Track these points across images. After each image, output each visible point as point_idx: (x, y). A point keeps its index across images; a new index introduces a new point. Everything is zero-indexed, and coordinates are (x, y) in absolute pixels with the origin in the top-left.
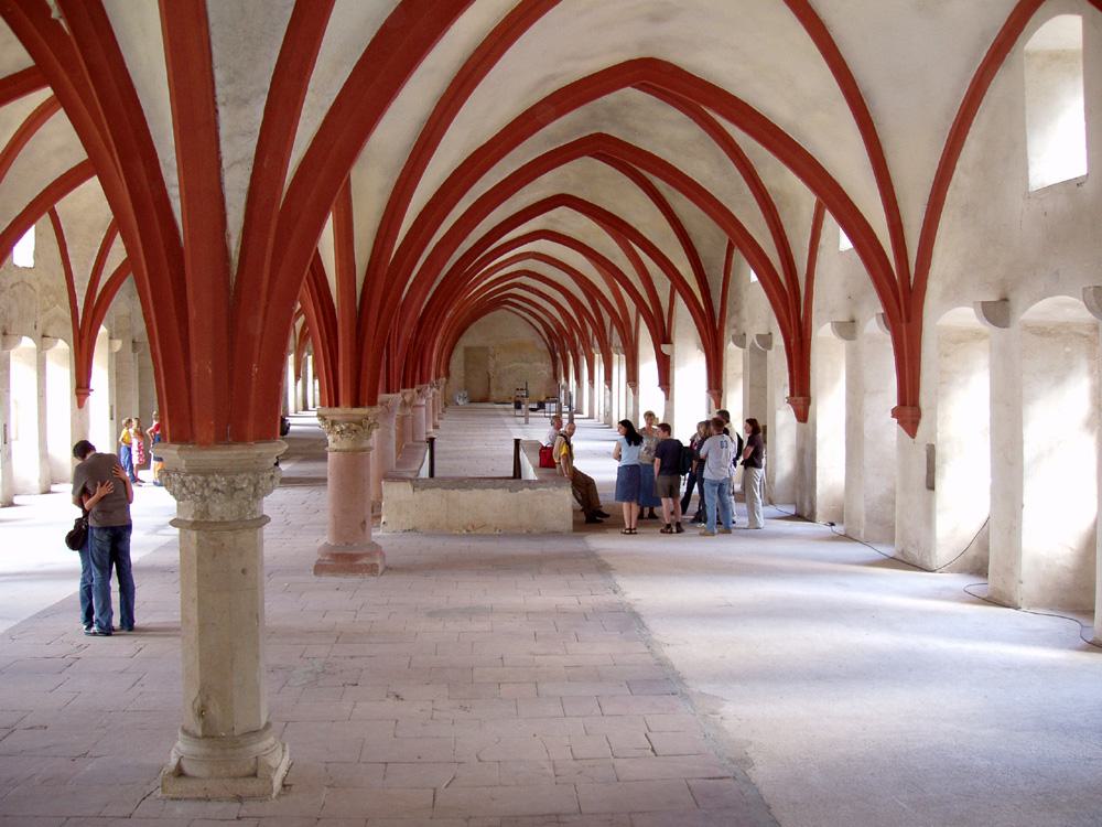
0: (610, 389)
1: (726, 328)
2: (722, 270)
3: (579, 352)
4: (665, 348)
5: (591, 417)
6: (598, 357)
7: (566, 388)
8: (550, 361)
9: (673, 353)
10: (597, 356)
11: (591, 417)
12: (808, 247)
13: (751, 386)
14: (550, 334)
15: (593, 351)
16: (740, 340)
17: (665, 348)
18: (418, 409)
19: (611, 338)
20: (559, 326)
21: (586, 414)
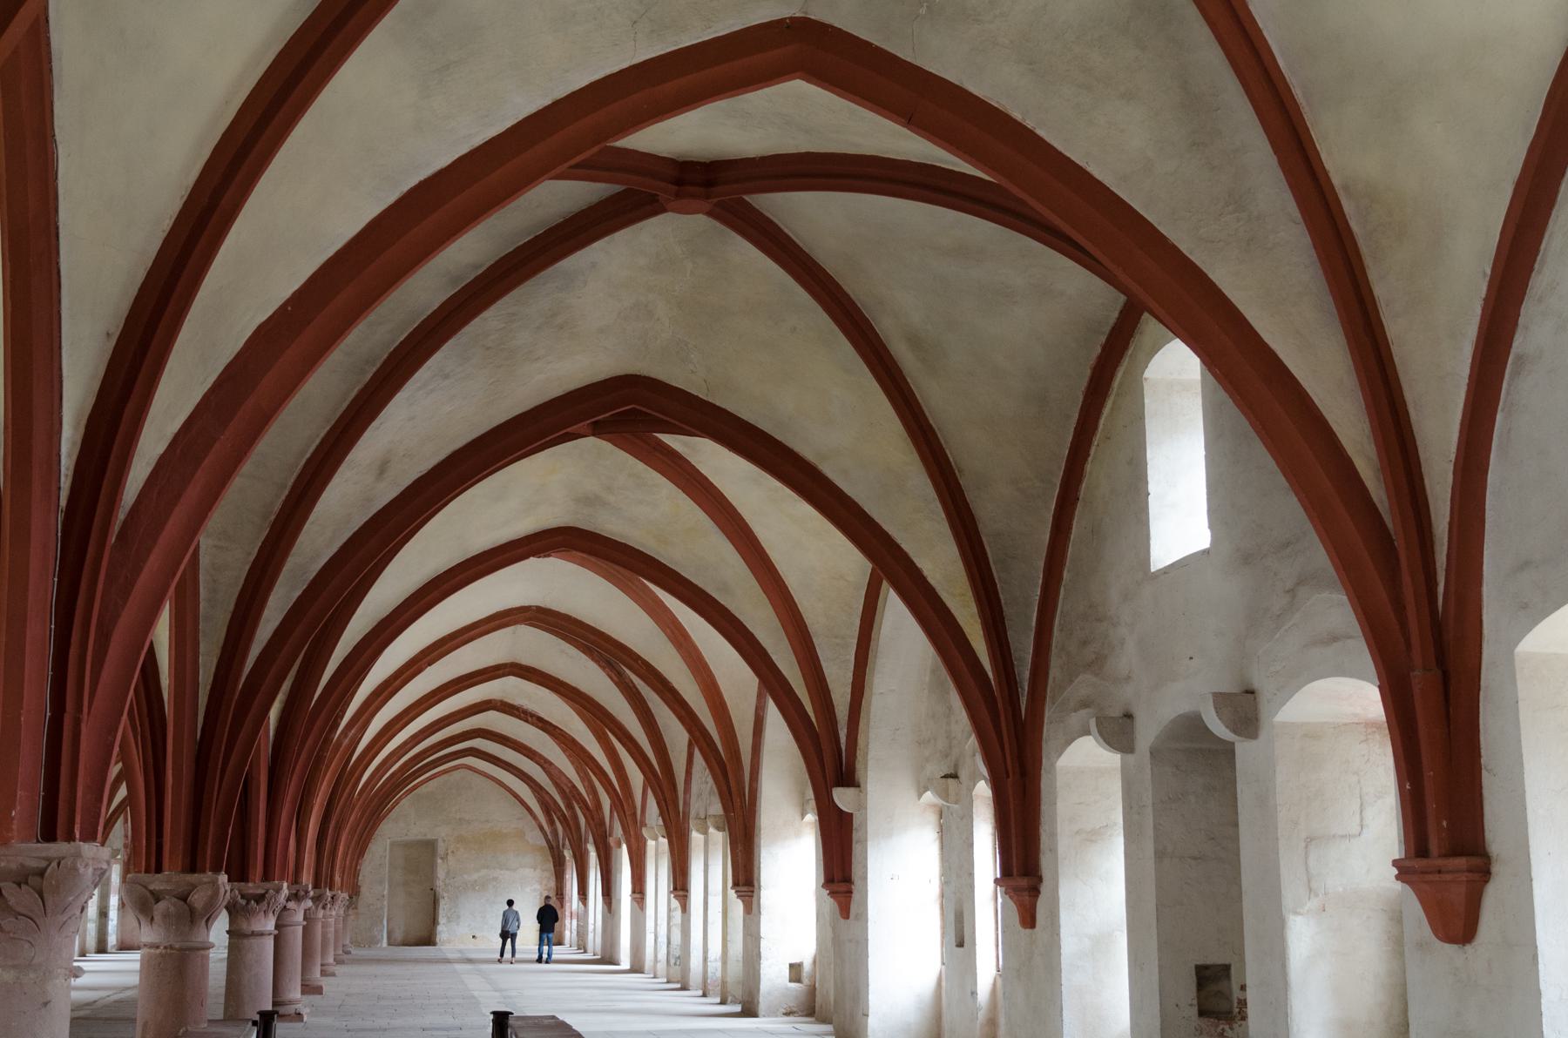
0: (685, 908)
1: (1049, 713)
2: (1041, 564)
4: (843, 798)
5: (637, 968)
6: (657, 851)
7: (582, 918)
8: (551, 866)
9: (862, 806)
10: (651, 844)
11: (637, 968)
12: (1465, 371)
13: (1160, 855)
15: (645, 832)
16: (1118, 733)
17: (843, 798)
18: (253, 941)
19: (687, 804)
20: (570, 793)
21: (625, 964)
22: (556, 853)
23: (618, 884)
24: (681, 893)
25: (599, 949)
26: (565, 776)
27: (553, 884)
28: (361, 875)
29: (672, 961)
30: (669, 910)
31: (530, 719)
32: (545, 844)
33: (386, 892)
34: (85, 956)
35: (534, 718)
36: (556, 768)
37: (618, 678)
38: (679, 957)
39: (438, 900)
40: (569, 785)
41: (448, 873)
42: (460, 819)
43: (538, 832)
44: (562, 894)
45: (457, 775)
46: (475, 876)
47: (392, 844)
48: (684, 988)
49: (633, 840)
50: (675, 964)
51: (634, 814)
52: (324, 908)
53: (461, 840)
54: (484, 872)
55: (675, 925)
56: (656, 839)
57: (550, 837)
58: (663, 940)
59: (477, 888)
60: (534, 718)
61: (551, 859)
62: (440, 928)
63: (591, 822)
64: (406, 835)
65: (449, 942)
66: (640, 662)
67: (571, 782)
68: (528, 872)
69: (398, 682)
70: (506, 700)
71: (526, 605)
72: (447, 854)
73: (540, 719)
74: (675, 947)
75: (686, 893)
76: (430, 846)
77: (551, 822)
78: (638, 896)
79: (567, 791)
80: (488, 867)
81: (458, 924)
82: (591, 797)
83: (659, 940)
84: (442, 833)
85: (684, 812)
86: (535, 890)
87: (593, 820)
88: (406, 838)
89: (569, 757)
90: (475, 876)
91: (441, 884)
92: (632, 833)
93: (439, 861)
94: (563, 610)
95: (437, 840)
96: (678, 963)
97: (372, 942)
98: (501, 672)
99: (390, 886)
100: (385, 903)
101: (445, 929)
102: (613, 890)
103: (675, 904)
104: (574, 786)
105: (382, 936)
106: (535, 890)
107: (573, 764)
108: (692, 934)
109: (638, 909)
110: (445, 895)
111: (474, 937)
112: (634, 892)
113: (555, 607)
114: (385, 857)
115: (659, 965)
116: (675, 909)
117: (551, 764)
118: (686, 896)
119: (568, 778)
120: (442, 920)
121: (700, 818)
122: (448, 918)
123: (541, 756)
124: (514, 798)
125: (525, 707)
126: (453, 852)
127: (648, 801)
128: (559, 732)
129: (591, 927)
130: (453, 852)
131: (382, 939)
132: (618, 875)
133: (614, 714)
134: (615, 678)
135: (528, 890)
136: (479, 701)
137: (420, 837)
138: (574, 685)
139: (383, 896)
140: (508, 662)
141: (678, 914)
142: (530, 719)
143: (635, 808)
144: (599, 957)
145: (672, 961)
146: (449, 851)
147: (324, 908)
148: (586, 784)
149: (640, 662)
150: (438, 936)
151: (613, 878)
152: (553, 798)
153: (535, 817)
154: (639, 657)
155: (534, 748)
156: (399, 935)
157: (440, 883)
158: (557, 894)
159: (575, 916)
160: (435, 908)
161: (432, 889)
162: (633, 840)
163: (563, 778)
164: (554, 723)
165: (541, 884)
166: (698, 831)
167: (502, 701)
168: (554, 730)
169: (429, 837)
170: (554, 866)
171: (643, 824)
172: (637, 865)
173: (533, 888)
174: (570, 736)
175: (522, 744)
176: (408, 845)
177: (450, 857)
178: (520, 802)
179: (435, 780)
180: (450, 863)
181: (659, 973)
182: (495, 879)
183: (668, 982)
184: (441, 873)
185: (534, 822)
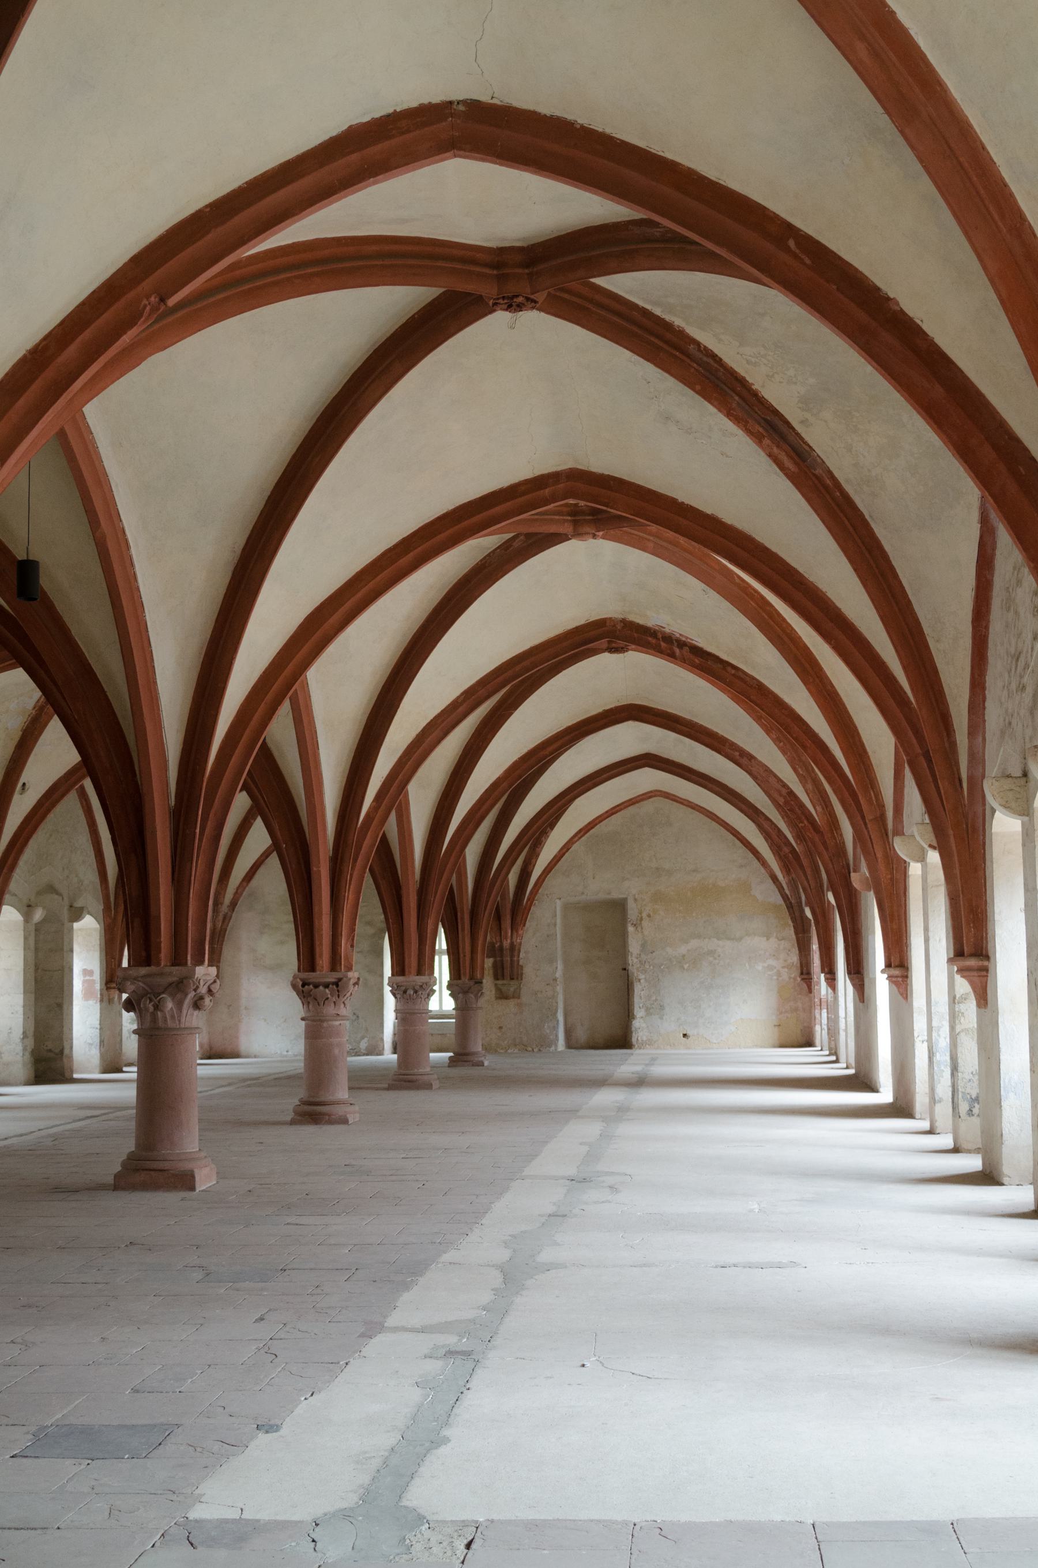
0: (984, 995)
3: (855, 879)
8: (790, 932)
10: (915, 869)
14: (788, 859)
15: (900, 847)
19: (977, 759)
20: (788, 803)
22: (797, 914)
23: (867, 950)
24: (972, 962)
25: (852, 1061)
26: (775, 776)
27: (794, 958)
28: (522, 951)
29: (964, 1107)
30: (953, 1000)
31: (677, 651)
32: (780, 901)
33: (559, 974)
34: (120, 1071)
35: (686, 649)
36: (764, 765)
37: (796, 463)
38: (977, 1099)
39: (632, 983)
40: (784, 791)
41: (643, 946)
42: (657, 869)
43: (773, 887)
44: (809, 973)
45: (648, 806)
46: (683, 949)
47: (566, 907)
48: (988, 1177)
49: (881, 866)
50: (970, 1112)
51: (882, 818)
52: (197, 1005)
53: (658, 898)
54: (694, 943)
55: (966, 1031)
56: (922, 859)
57: (787, 892)
58: (943, 1057)
59: (686, 966)
60: (686, 649)
61: (790, 922)
62: (636, 1023)
63: (825, 853)
64: (583, 893)
65: (650, 1043)
66: (791, 243)
67: (785, 785)
68: (758, 942)
69: (72, 351)
70: (632, 618)
71: (436, 99)
72: (641, 919)
73: (697, 651)
74: (968, 1077)
75: (986, 963)
76: (618, 907)
77: (786, 868)
78: (896, 972)
79: (781, 801)
80: (699, 937)
81: (661, 1018)
82: (819, 808)
83: (938, 1057)
84: (632, 889)
85: (970, 778)
86: (770, 968)
87: (827, 849)
88: (584, 897)
89: (776, 741)
90: (683, 949)
91: (635, 960)
92: (879, 855)
93: (631, 929)
94: (545, 109)
95: (625, 900)
96: (976, 1111)
97: (544, 1043)
98: (547, 492)
99: (566, 962)
100: (560, 989)
101: (644, 1025)
102: (865, 964)
103: (963, 986)
104: (791, 793)
105: (557, 1036)
106: (770, 968)
107: (784, 752)
108: (1004, 1057)
109: (900, 997)
110: (641, 976)
111: (685, 1035)
112: (888, 965)
113: (523, 99)
114: (555, 925)
115: (938, 1108)
116: (964, 998)
117: (751, 757)
118: (986, 970)
119: (779, 780)
120: (639, 1012)
121: (1009, 776)
122: (647, 1010)
123: (733, 746)
124: (732, 836)
125: (667, 630)
126: (649, 916)
127: (906, 791)
128: (733, 672)
129: (842, 1025)
130: (649, 916)
131: (557, 1039)
132: (870, 937)
133: (801, 570)
134: (788, 464)
135: (760, 968)
136: (582, 622)
137: (602, 896)
138: (709, 510)
139: (555, 980)
140: (559, 469)
141: (970, 1008)
142: (677, 651)
143: (882, 806)
144: (852, 1071)
145: (964, 1107)
146: (644, 915)
147: (197, 1005)
148: (810, 786)
149: (791, 243)
150: (634, 1034)
151: (864, 944)
152: (776, 826)
153: (764, 863)
154: (789, 229)
155: (721, 732)
156: (581, 1034)
157: (633, 961)
158: (802, 973)
159: (824, 1005)
160: (628, 999)
161: (625, 969)
162: (881, 866)
163: (772, 780)
164: (724, 657)
165: (778, 959)
166: (1007, 807)
167: (624, 621)
168: (724, 669)
169: (616, 895)
170: (796, 933)
171: (899, 832)
172: (892, 916)
173: (766, 965)
174: (754, 678)
175: (701, 726)
176: (589, 907)
177: (645, 923)
178: (742, 842)
179: (619, 813)
180: (646, 933)
181: (940, 1125)
182: (711, 953)
183: (956, 1150)
184: (634, 946)
185: (763, 870)
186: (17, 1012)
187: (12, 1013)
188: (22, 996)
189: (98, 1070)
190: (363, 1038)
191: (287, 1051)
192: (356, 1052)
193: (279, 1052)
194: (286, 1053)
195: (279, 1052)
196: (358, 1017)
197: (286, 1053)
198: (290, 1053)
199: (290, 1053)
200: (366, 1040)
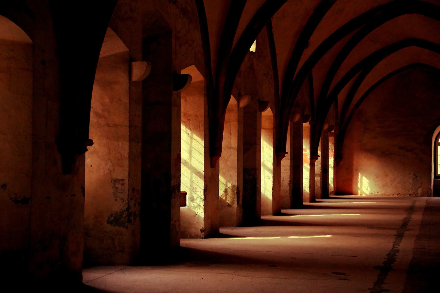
186: (287, 169)
187: (284, 170)
188: (289, 161)
189: (308, 201)
190: (419, 187)
191: (378, 193)
192: (416, 195)
193: (373, 193)
194: (377, 194)
195: (373, 193)
196: (417, 176)
197: (377, 194)
198: (379, 194)
199: (379, 194)
200: (421, 188)
